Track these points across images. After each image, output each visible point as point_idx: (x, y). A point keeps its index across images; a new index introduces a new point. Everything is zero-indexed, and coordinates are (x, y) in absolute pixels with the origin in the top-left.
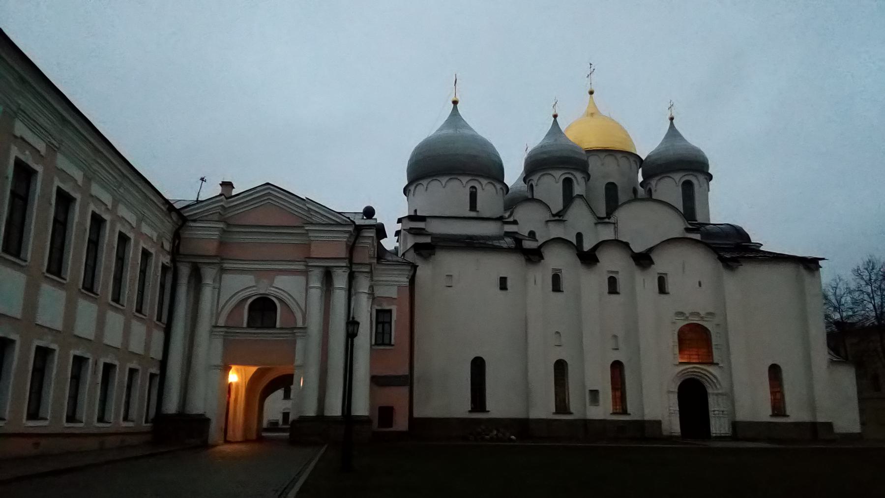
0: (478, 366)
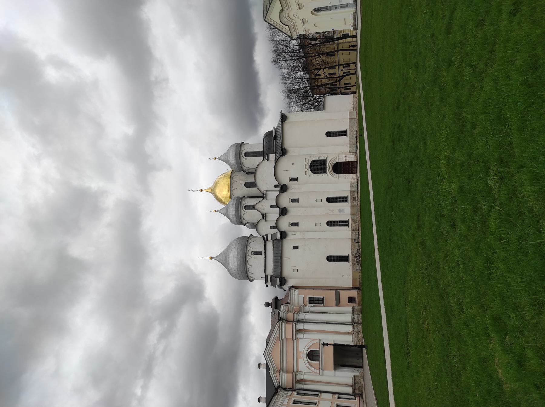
0: (330, 259)
